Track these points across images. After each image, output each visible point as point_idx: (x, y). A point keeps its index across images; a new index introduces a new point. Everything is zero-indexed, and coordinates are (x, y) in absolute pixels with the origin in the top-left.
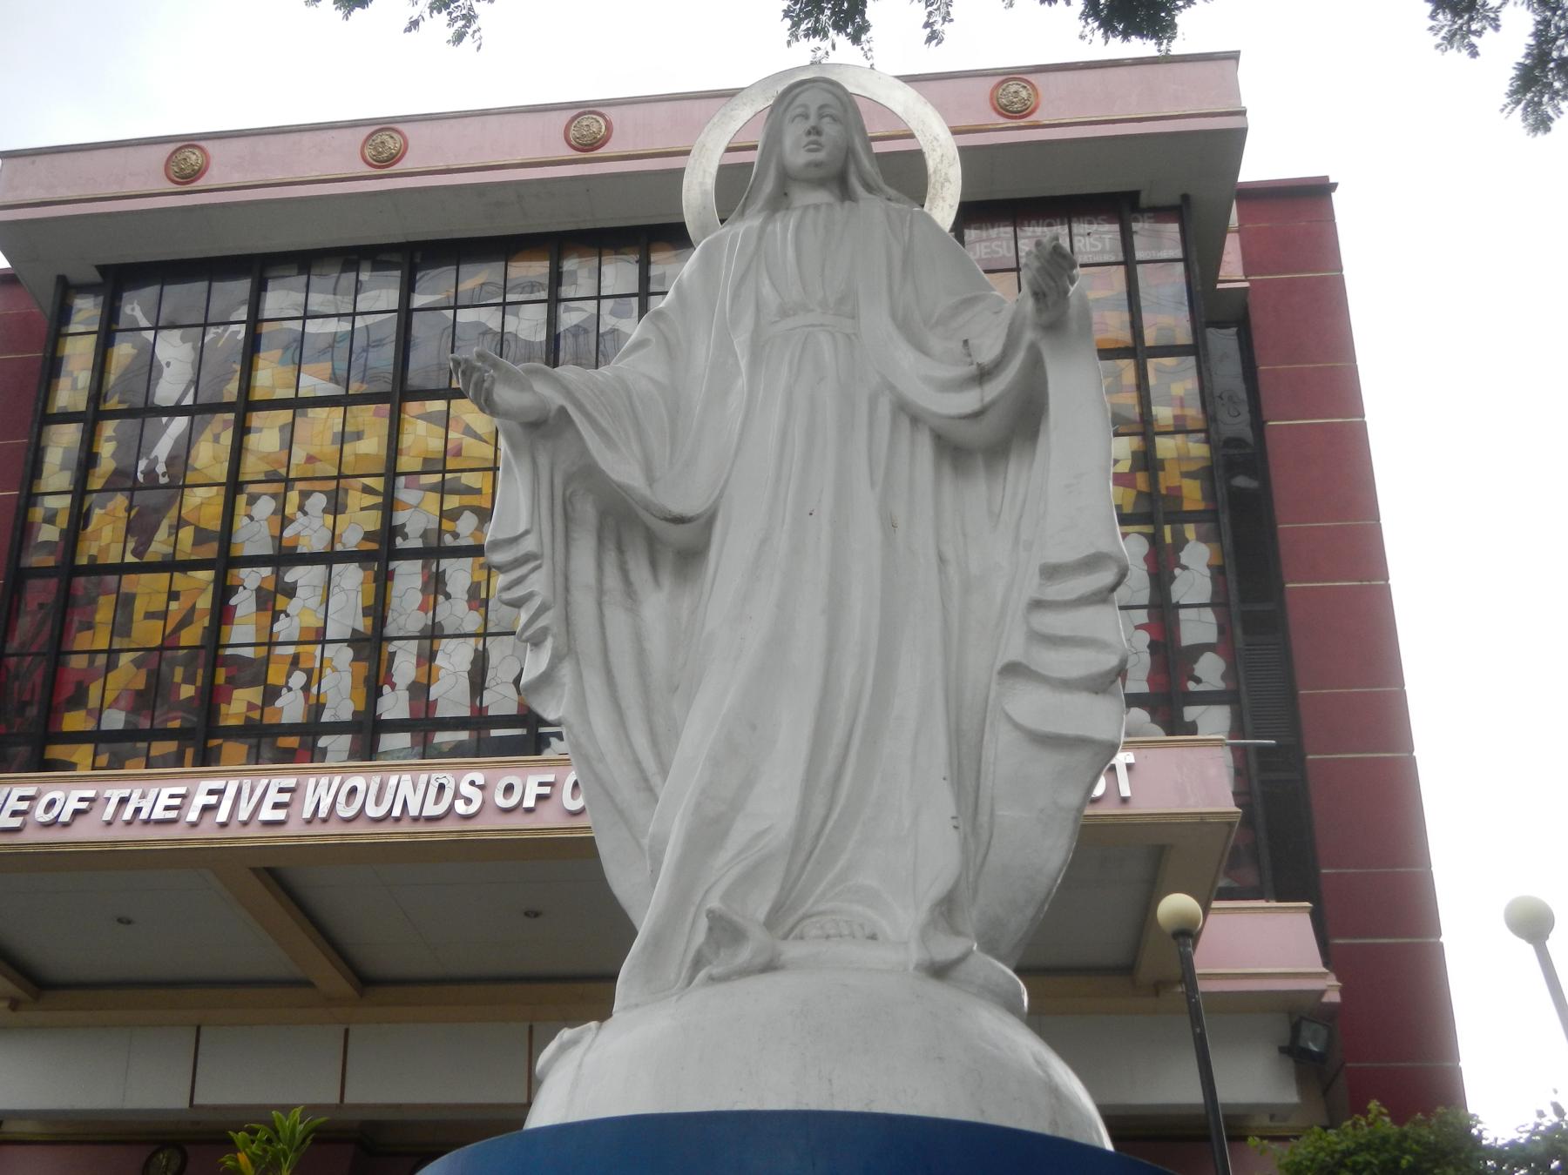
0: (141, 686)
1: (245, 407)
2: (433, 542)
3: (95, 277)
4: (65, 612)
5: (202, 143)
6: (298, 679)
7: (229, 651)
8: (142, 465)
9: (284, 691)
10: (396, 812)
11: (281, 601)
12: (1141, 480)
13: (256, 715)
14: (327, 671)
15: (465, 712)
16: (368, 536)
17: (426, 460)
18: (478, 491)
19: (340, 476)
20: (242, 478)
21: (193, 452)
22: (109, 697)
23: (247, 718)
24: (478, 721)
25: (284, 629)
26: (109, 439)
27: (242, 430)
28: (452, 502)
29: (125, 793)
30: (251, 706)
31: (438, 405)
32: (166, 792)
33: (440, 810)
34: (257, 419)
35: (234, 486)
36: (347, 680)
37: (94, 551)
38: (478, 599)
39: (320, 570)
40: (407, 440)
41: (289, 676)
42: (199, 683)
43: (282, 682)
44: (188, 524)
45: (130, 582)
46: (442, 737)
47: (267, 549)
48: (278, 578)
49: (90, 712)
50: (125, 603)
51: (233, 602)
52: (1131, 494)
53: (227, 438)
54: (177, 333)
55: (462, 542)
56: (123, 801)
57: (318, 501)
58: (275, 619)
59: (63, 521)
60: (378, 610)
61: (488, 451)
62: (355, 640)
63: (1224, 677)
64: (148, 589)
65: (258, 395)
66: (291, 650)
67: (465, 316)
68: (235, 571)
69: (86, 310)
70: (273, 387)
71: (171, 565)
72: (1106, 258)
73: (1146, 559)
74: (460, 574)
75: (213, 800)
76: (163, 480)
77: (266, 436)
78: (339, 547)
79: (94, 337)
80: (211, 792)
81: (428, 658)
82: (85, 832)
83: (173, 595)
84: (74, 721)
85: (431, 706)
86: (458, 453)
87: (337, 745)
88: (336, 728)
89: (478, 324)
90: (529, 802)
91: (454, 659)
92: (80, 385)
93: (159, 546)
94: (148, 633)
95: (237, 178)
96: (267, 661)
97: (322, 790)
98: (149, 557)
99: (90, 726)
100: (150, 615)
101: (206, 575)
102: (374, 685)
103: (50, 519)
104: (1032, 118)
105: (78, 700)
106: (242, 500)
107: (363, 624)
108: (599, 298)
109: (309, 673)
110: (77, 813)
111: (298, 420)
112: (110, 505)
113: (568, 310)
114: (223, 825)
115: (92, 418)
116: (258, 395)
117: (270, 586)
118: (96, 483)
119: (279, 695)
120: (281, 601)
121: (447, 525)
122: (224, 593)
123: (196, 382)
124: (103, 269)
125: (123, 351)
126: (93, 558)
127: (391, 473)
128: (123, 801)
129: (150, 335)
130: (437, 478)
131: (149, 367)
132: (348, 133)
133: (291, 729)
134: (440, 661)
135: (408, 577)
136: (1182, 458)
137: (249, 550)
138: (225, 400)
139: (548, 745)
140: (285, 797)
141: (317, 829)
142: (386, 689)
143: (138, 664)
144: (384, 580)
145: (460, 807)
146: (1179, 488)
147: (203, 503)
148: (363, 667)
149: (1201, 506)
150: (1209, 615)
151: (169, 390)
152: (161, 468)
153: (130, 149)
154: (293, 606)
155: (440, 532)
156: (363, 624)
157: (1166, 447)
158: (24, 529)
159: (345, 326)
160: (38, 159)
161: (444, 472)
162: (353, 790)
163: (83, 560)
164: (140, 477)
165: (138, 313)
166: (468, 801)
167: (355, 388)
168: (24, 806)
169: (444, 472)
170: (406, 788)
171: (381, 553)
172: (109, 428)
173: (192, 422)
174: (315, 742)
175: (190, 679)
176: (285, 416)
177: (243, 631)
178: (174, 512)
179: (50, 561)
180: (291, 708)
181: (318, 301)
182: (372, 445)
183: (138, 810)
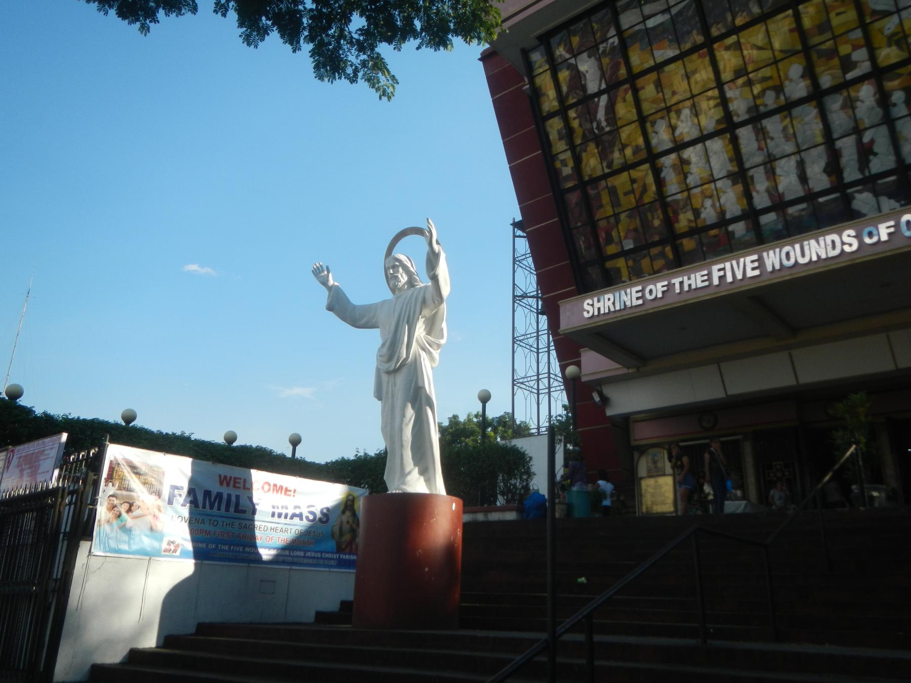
1: (633, 78)
2: (755, 114)
3: (537, 42)
4: (589, 205)
7: (669, 199)
9: (703, 210)
11: (685, 167)
13: (693, 225)
14: (721, 194)
15: (801, 193)
16: (718, 122)
18: (771, 78)
19: (693, 97)
20: (646, 114)
22: (622, 234)
23: (690, 227)
24: (810, 197)
25: (691, 180)
26: (575, 118)
27: (636, 91)
29: (680, 279)
31: (733, 39)
32: (698, 275)
33: (837, 252)
34: (640, 82)
35: (642, 120)
37: (589, 173)
39: (699, 147)
40: (721, 66)
42: (661, 217)
44: (627, 145)
45: (611, 181)
47: (670, 145)
50: (613, 191)
51: (662, 175)
53: (629, 96)
54: (585, 55)
56: (681, 283)
57: (686, 112)
58: (686, 177)
59: (571, 164)
60: (737, 156)
62: (730, 176)
64: (621, 181)
65: (636, 70)
68: (657, 161)
70: (642, 63)
71: (627, 167)
74: (772, 125)
75: (722, 273)
76: (607, 129)
77: (648, 91)
78: (705, 133)
79: (549, 72)
80: (719, 270)
81: (771, 174)
82: (671, 301)
83: (633, 181)
84: (611, 249)
85: (781, 196)
87: (739, 229)
88: (735, 220)
96: (689, 197)
98: (615, 167)
99: (619, 249)
100: (626, 194)
101: (646, 166)
102: (748, 195)
103: (564, 163)
105: (609, 240)
106: (648, 125)
110: (663, 292)
112: (588, 149)
114: (731, 283)
115: (562, 112)
116: (636, 70)
117: (677, 162)
118: (578, 141)
121: (759, 102)
122: (657, 172)
123: (603, 76)
124: (539, 38)
126: (590, 176)
128: (681, 283)
131: (577, 78)
135: (745, 134)
137: (661, 149)
138: (622, 79)
139: (854, 198)
140: (756, 264)
142: (754, 194)
144: (735, 142)
145: (847, 249)
147: (630, 134)
148: (740, 187)
152: (604, 124)
155: (756, 107)
158: (554, 175)
159: (667, 17)
162: (788, 254)
163: (587, 178)
164: (596, 131)
165: (564, 53)
166: (850, 245)
168: (640, 294)
169: (747, 74)
171: (728, 127)
172: (572, 114)
174: (727, 230)
176: (653, 76)
177: (673, 186)
178: (618, 143)
180: (709, 214)
182: (704, 75)
183: (690, 285)
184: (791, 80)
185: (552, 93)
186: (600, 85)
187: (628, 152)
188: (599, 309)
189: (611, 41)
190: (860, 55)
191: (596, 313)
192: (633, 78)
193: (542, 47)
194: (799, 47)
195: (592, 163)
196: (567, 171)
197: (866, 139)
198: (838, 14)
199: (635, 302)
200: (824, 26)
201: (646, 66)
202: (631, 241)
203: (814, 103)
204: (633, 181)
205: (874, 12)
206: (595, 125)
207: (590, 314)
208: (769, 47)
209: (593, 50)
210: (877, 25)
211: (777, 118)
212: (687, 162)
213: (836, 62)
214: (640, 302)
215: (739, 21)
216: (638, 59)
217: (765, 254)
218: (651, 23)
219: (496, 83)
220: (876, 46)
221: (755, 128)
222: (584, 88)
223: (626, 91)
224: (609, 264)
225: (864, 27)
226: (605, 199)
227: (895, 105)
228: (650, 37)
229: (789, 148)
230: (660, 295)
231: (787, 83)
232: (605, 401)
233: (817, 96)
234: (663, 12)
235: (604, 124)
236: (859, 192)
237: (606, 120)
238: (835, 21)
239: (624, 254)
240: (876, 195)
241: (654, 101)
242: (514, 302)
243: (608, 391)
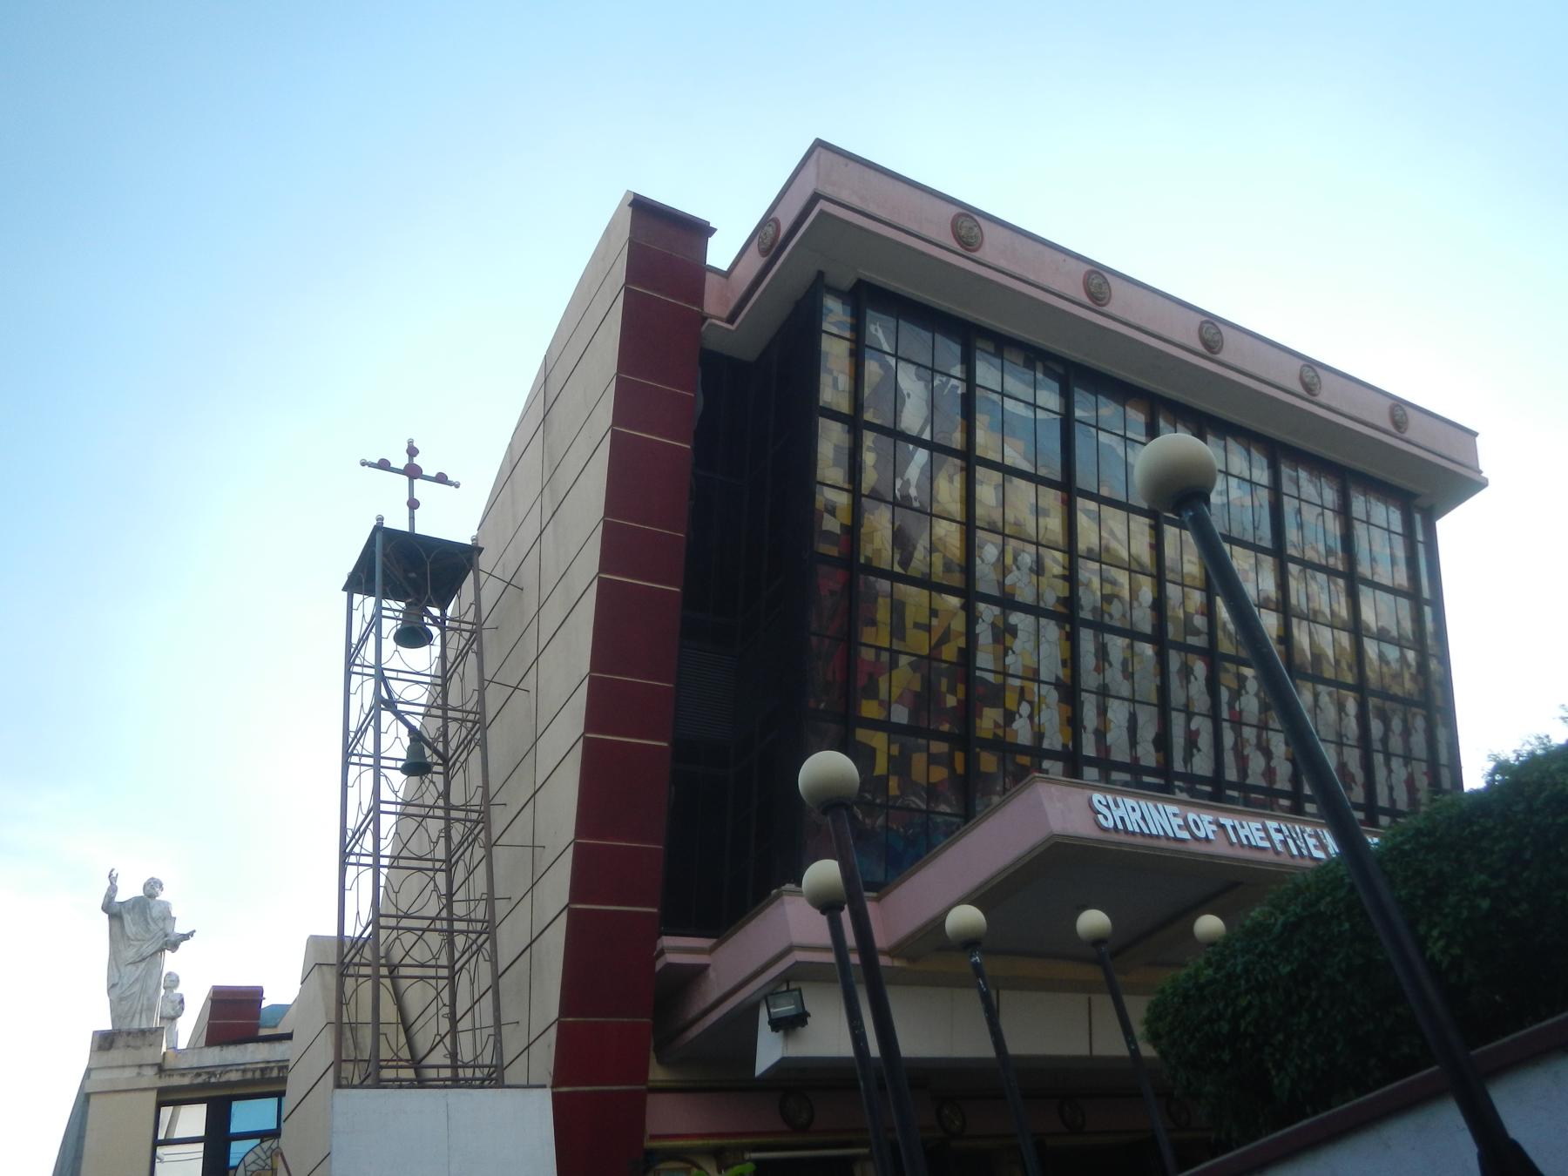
0: (917, 687)
2: (1098, 619)
6: (1025, 709)
7: (978, 673)
13: (1000, 732)
22: (896, 692)
23: (995, 734)
30: (996, 725)
36: (1056, 719)
41: (1019, 704)
43: (1014, 708)
46: (1115, 776)
48: (1005, 617)
49: (881, 703)
50: (898, 608)
55: (1118, 624)
58: (1006, 654)
59: (844, 517)
60: (1072, 661)
62: (1058, 684)
66: (1017, 683)
69: (835, 314)
81: (1102, 711)
83: (933, 613)
85: (1107, 750)
87: (1054, 767)
88: (1052, 755)
91: (1118, 713)
94: (919, 642)
98: (911, 572)
100: (917, 625)
102: (1074, 723)
105: (872, 693)
107: (1061, 673)
109: (1031, 703)
119: (1013, 720)
122: (972, 619)
126: (867, 558)
129: (892, 361)
132: (1072, 262)
133: (1024, 750)
134: (1110, 715)
143: (913, 667)
144: (1072, 639)
148: (1068, 710)
154: (1018, 645)
156: (1061, 673)
159: (1029, 413)
160: (852, 164)
165: (880, 335)
175: (953, 691)
181: (1012, 385)
190: (1200, 622)
196: (831, 524)
197: (1193, 726)
204: (933, 613)
209: (930, 371)
212: (1013, 631)
221: (1096, 636)
226: (883, 614)
229: (1125, 690)
236: (1182, 790)
237: (918, 487)
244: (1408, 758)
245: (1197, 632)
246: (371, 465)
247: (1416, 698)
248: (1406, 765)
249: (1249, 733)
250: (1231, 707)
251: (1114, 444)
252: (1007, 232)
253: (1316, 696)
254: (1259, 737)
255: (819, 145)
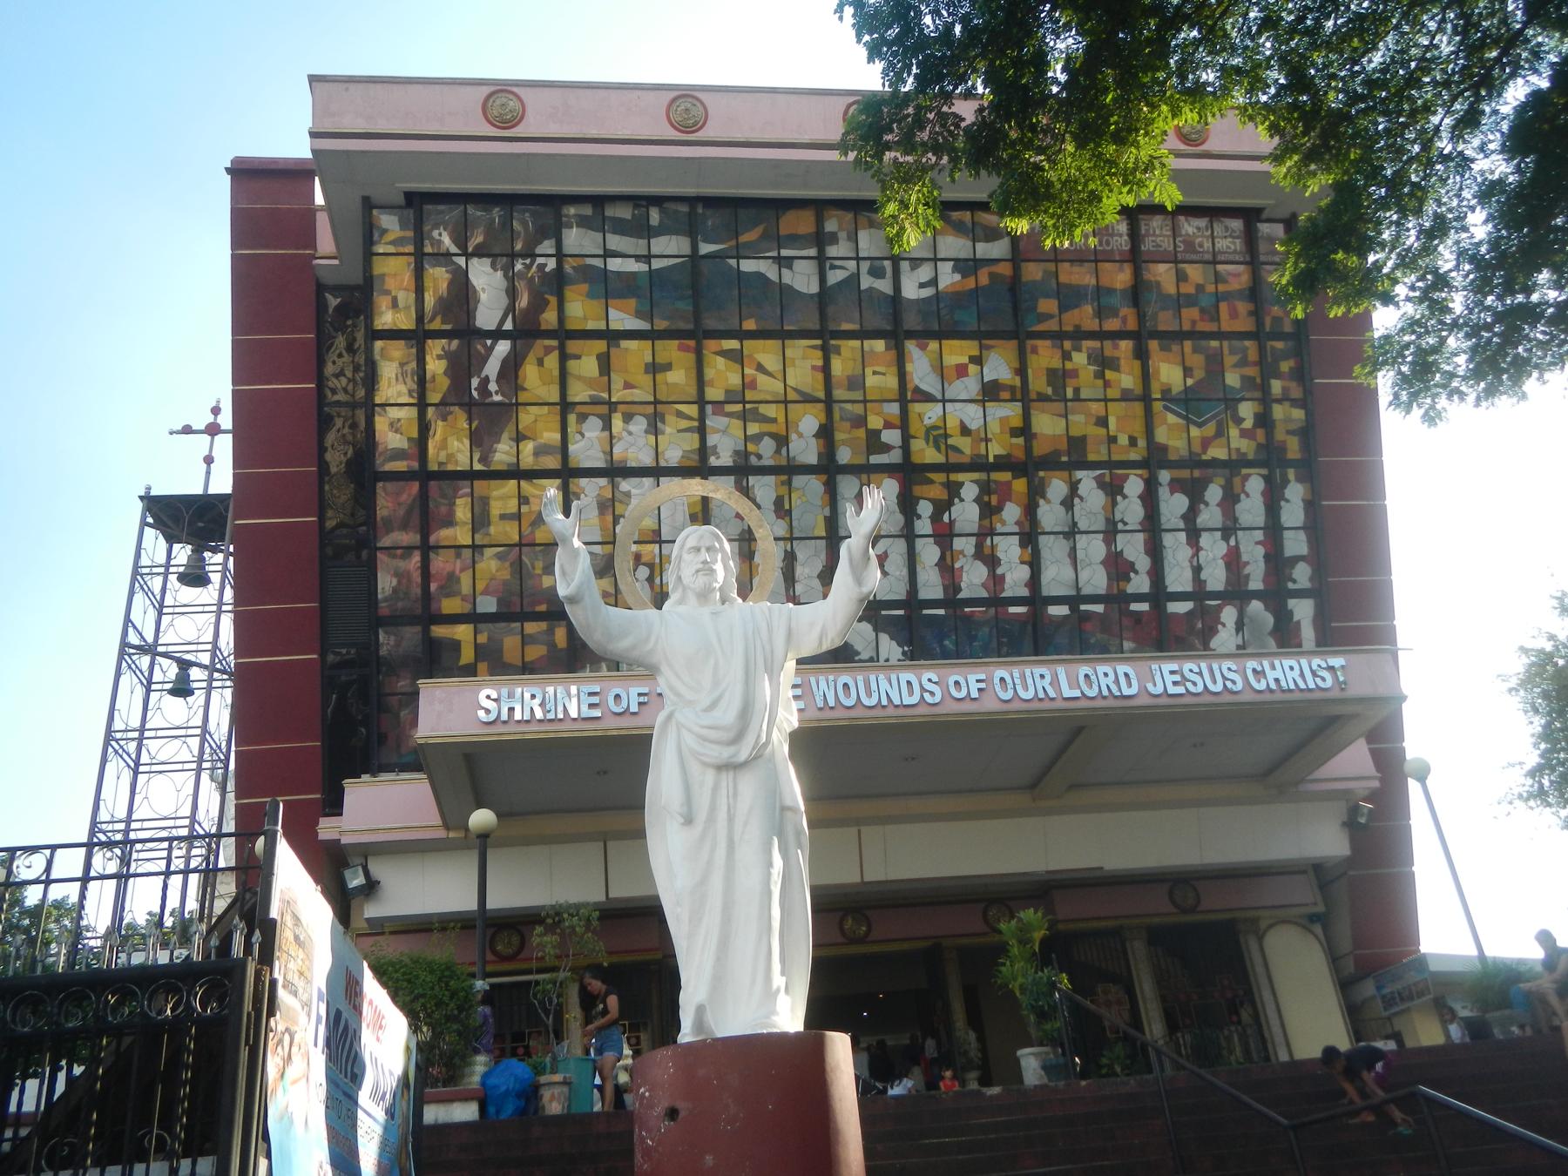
2: (741, 462)
3: (401, 200)
5: (515, 90)
6: (643, 572)
8: (475, 382)
10: (884, 702)
12: (1260, 433)
17: (727, 392)
18: (774, 420)
19: (656, 402)
21: (520, 373)
22: (480, 586)
28: (754, 428)
31: (733, 344)
33: (915, 699)
34: (573, 346)
38: (782, 509)
40: (709, 373)
44: (525, 438)
47: (600, 464)
52: (1253, 444)
53: (552, 361)
54: (487, 261)
55: (767, 462)
57: (639, 425)
58: (615, 522)
61: (779, 386)
63: (1311, 579)
67: (748, 266)
70: (585, 318)
71: (516, 473)
72: (1237, 258)
73: (1264, 494)
76: (497, 398)
77: (586, 365)
86: (753, 385)
89: (760, 276)
90: (975, 694)
92: (401, 304)
93: (503, 453)
95: (553, 130)
97: (823, 684)
99: (467, 608)
104: (1205, 147)
106: (572, 418)
108: (858, 259)
109: (651, 566)
111: (613, 351)
113: (833, 267)
115: (418, 337)
118: (434, 397)
120: (619, 509)
123: (511, 308)
125: (438, 277)
126: (440, 464)
127: (701, 401)
129: (461, 261)
130: (739, 407)
131: (462, 295)
132: (652, 94)
136: (1288, 420)
138: (543, 327)
141: (828, 714)
146: (1284, 442)
149: (1298, 456)
150: (1302, 535)
151: (488, 314)
153: (446, 88)
155: (746, 454)
157: (1278, 411)
159: (643, 267)
160: (352, 87)
161: (744, 402)
164: (475, 394)
165: (447, 240)
166: (932, 694)
167: (661, 324)
168: (595, 700)
170: (884, 685)
173: (514, 347)
176: (601, 346)
179: (400, 466)
182: (679, 377)
184: (801, 435)
185: (406, 298)
186: (502, 321)
187: (528, 447)
188: (511, 710)
189: (540, 260)
190: (892, 437)
191: (504, 716)
192: (564, 335)
193: (410, 213)
194: (821, 395)
195: (452, 446)
198: (875, 373)
199: (586, 713)
200: (857, 383)
201: (591, 325)
202: (494, 600)
203: (824, 477)
205: (917, 390)
206: (475, 382)
207: (492, 717)
208: (780, 376)
210: (916, 408)
211: (770, 480)
213: (861, 433)
214: (597, 713)
215: (750, 325)
216: (580, 309)
217: (813, 680)
218: (615, 264)
219: (246, 228)
220: (912, 431)
222: (470, 314)
223: (548, 350)
224: (439, 631)
225: (903, 401)
226: (462, 511)
227: (919, 517)
228: (608, 287)
230: (634, 708)
231: (793, 436)
232: (371, 887)
233: (828, 469)
234: (638, 258)
235: (493, 387)
238: (871, 381)
239: (473, 618)
240: (876, 630)
241: (590, 383)
242: (122, 654)
243: (378, 868)
244: (1229, 529)
245: (887, 448)
246: (178, 432)
247: (1251, 456)
248: (1226, 538)
249: (965, 545)
250: (936, 518)
251: (763, 270)
252: (557, 92)
253: (1074, 487)
254: (979, 547)
255: (313, 79)
